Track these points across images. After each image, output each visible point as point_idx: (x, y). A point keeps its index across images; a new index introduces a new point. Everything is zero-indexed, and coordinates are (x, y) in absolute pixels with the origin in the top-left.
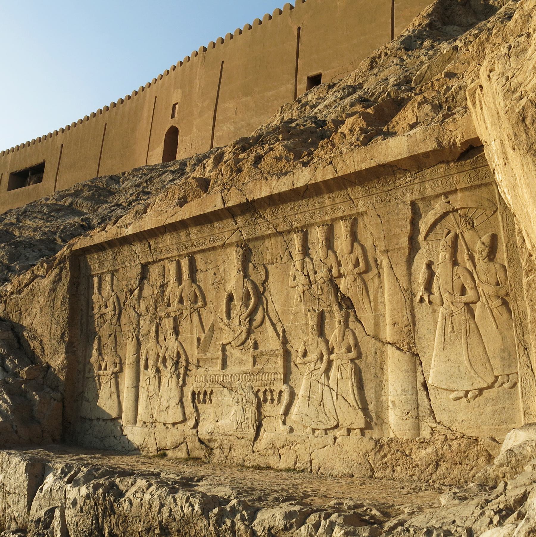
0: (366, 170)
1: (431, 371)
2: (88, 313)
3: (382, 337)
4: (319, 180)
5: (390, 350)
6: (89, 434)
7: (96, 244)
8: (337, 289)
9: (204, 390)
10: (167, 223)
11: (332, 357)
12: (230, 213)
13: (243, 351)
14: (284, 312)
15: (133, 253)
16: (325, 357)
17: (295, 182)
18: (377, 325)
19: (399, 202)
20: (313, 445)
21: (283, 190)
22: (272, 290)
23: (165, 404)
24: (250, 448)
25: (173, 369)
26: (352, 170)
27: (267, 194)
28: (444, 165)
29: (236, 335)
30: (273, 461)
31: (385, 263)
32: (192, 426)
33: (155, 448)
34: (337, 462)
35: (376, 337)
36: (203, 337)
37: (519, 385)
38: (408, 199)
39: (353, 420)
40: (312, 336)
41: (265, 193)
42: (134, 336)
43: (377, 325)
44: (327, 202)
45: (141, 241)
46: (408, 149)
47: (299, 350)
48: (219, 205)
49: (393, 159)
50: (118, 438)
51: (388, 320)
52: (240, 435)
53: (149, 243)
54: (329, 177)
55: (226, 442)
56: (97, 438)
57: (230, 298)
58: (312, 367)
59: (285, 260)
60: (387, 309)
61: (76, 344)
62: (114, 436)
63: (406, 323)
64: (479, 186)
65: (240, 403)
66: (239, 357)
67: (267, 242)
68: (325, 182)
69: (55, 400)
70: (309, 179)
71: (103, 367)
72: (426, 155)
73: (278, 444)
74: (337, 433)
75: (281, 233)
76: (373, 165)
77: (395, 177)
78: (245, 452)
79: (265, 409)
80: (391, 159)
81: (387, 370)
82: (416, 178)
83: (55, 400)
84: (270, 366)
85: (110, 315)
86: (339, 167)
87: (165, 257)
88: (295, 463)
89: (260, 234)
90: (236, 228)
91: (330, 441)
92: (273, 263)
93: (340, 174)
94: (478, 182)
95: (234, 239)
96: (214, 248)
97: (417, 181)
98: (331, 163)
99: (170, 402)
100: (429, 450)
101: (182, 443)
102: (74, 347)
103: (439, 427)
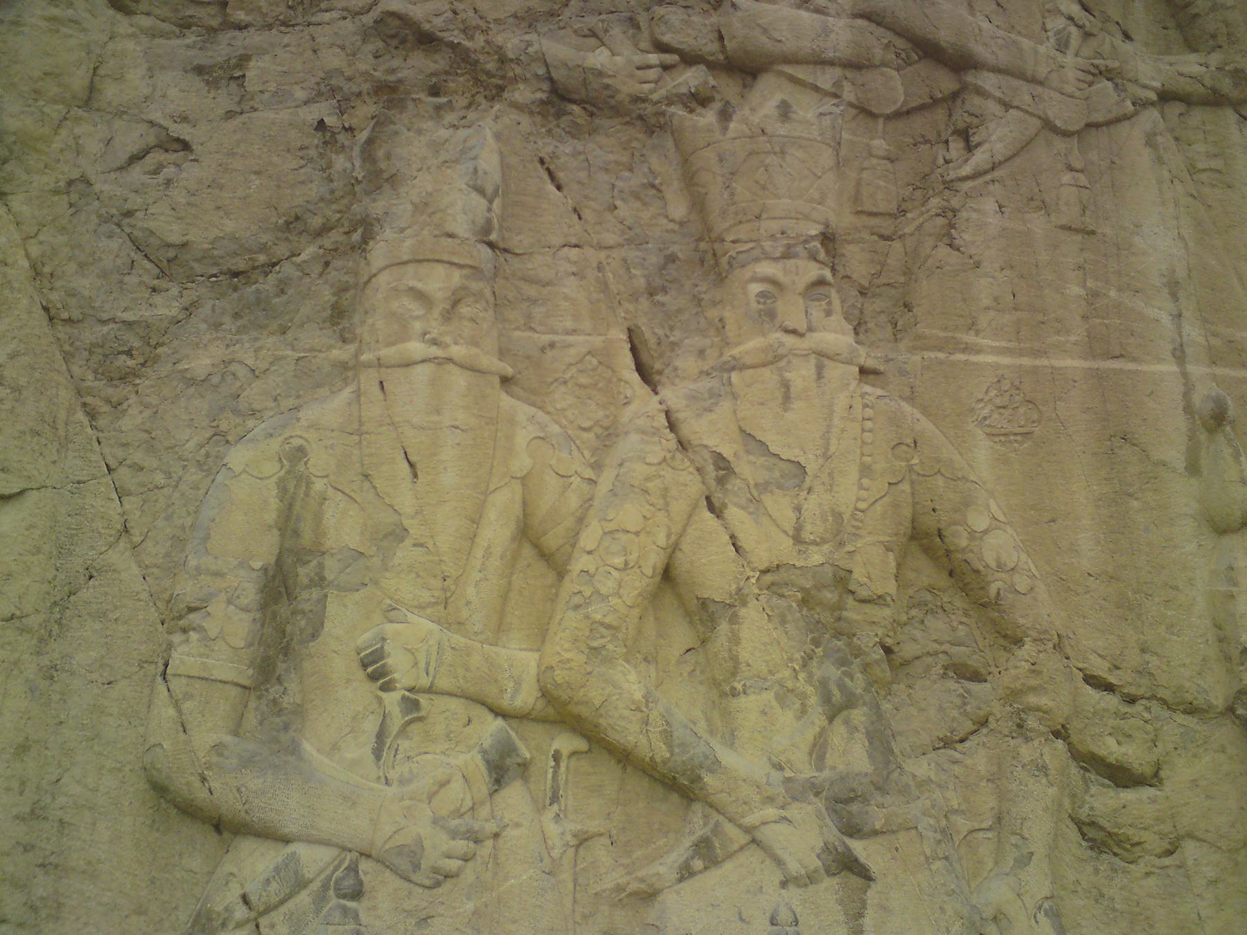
25: (851, 755)
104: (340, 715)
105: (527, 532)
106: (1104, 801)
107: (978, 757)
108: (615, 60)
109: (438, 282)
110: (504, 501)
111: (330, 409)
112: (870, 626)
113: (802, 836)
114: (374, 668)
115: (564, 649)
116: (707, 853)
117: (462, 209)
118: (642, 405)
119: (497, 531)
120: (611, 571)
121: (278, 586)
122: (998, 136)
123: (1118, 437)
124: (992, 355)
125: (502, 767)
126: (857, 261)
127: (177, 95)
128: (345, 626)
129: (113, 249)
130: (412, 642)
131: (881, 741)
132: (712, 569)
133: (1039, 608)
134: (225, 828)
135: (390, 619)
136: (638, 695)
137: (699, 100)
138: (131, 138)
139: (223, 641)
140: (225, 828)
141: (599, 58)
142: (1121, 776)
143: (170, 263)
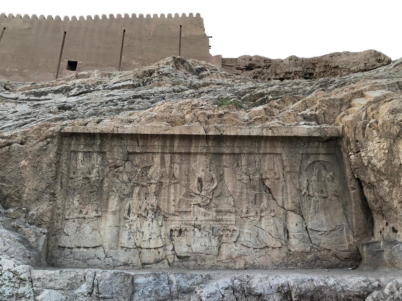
0: (289, 136)
1: (309, 223)
2: (68, 176)
3: (285, 208)
4: (265, 135)
5: (291, 214)
6: (70, 258)
7: (90, 133)
8: (264, 184)
9: (179, 228)
10: (162, 133)
11: (262, 215)
12: (207, 138)
13: (207, 209)
14: (233, 191)
15: (122, 144)
16: (259, 214)
17: (251, 133)
18: (283, 202)
19: (297, 153)
20: (255, 256)
21: (244, 135)
22: (226, 180)
23: (148, 237)
24: (215, 260)
25: (153, 217)
26: (282, 135)
27: (235, 134)
28: (317, 143)
29: (204, 200)
30: (231, 265)
31: (288, 176)
32: (171, 249)
33: (140, 263)
34: (269, 263)
35: (284, 208)
36: (178, 199)
37: (344, 229)
38: (301, 152)
39: (275, 243)
40: (251, 204)
41: (233, 134)
42: (117, 194)
43: (283, 202)
44: (263, 145)
45: (131, 139)
46: (308, 133)
47: (243, 211)
48: (202, 132)
49: (301, 135)
50: (102, 259)
51: (290, 201)
52: (208, 253)
53: (138, 141)
54: (270, 135)
55: (198, 257)
56: (79, 260)
57: (200, 180)
58: (252, 219)
59: (234, 167)
60: (289, 196)
61: (57, 195)
62: (98, 258)
63: (298, 202)
64: (329, 154)
65: (207, 236)
66: (205, 212)
67: (224, 157)
68: (267, 137)
69: (44, 234)
70: (259, 133)
71: (84, 213)
72: (315, 137)
73: (234, 257)
74: (267, 250)
75: (234, 154)
76: (292, 135)
77: (297, 142)
78: (212, 261)
79: (223, 239)
80: (300, 135)
81: (289, 222)
82: (305, 145)
83: (44, 234)
84: (226, 217)
85: (94, 179)
86: (275, 132)
87: (151, 151)
88: (245, 265)
89: (222, 151)
90: (207, 146)
91: (264, 254)
92: (227, 167)
93: (276, 135)
94: (328, 153)
95: (205, 151)
96: (189, 154)
97: (305, 146)
98: (270, 129)
99: (152, 235)
100: (312, 255)
101: (164, 259)
102: (56, 197)
103: (314, 246)
104: (131, 215)
105: (139, 207)
106: (165, 219)
107: (159, 217)
108: (145, 184)
109: (136, 195)
110: (139, 205)
111: (131, 201)
112: (155, 210)
113: (150, 220)
114: (133, 213)
115: (141, 212)
116: (146, 220)
117: (137, 192)
118: (145, 200)
119: (138, 207)
120: (143, 208)
121: (129, 209)
122: (164, 187)
123: (169, 202)
124: (163, 197)
125: (138, 217)
126: (156, 193)
127: (125, 187)
128: (132, 211)
129: (122, 194)
130: (134, 211)
131: (155, 216)
132: (148, 208)
133: (163, 210)
134: (127, 219)
135: (133, 210)
136: (144, 214)
137: (149, 186)
138: (123, 189)
139: (126, 212)
140: (127, 219)
141: (144, 184)
142: (166, 217)
143: (124, 195)
